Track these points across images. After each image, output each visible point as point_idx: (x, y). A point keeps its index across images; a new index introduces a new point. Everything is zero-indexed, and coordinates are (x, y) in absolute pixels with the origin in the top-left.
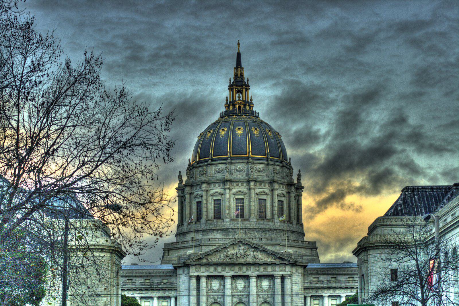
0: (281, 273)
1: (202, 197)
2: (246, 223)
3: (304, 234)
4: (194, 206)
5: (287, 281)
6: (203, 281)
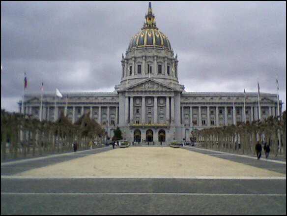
1: (132, 64)
2: (152, 75)
3: (178, 82)
4: (129, 69)
5: (172, 100)
6: (132, 100)
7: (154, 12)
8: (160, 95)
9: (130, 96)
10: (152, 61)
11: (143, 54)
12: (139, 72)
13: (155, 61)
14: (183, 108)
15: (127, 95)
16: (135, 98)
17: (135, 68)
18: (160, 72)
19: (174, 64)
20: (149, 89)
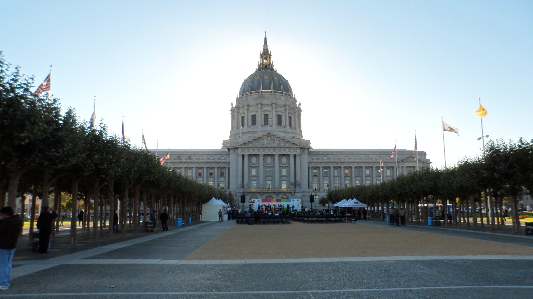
0: (294, 153)
4: (240, 119)
6: (246, 158)
7: (271, 50)
8: (282, 152)
9: (244, 153)
10: (270, 109)
11: (259, 102)
12: (254, 123)
13: (274, 109)
14: (310, 169)
15: (240, 152)
16: (250, 156)
17: (248, 120)
18: (280, 123)
19: (297, 113)
20: (269, 145)
